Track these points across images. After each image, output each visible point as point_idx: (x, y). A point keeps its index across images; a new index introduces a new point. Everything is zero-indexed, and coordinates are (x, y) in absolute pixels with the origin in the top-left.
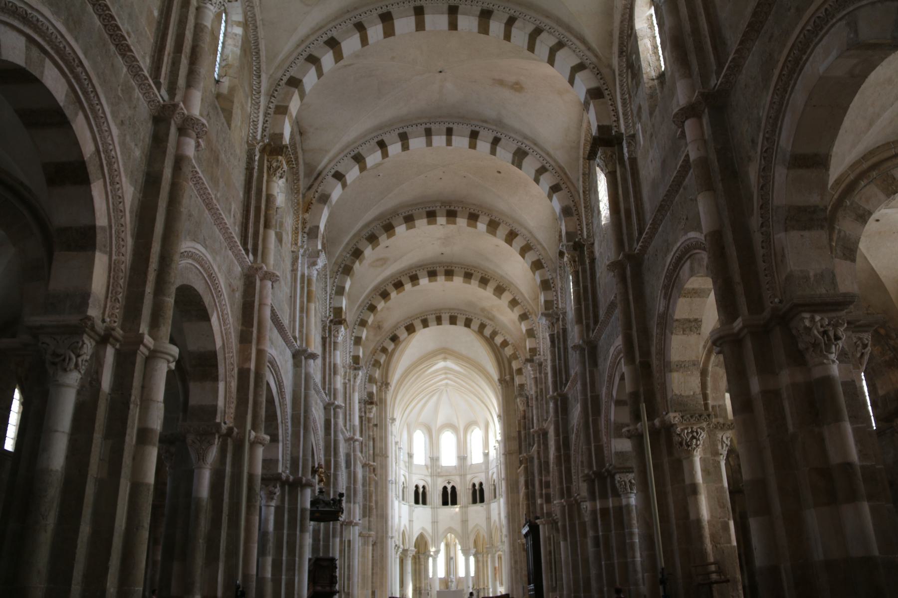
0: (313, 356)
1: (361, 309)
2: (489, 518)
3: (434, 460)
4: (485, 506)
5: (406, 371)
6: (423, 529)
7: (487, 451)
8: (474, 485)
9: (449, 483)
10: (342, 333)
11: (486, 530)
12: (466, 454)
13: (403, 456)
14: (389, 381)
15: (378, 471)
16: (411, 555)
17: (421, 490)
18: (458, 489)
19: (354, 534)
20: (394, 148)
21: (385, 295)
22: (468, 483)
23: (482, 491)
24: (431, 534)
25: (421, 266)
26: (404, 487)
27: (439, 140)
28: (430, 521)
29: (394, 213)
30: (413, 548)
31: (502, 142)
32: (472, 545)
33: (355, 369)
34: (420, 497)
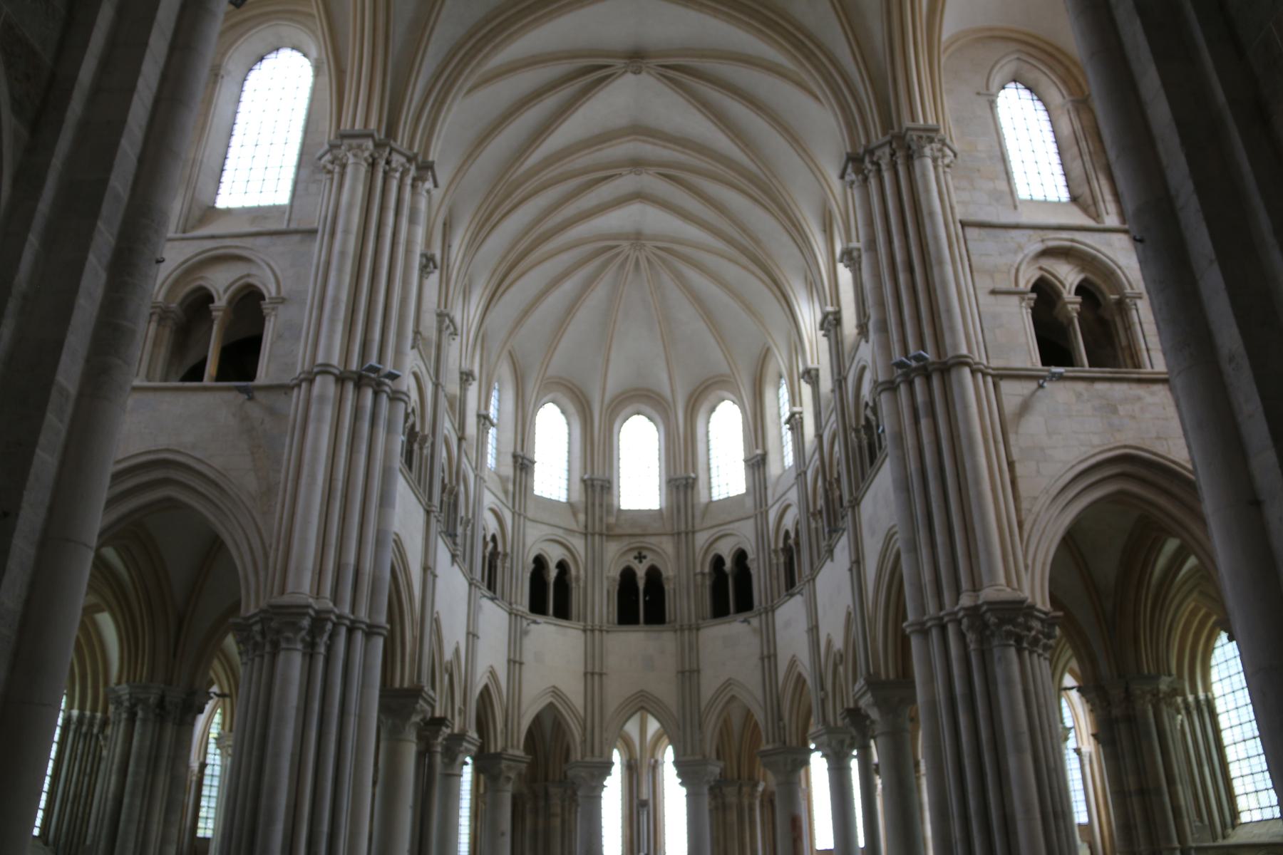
2: (769, 657)
4: (755, 622)
6: (555, 691)
7: (759, 452)
8: (718, 561)
9: (640, 558)
11: (759, 693)
12: (694, 469)
16: (512, 775)
17: (553, 573)
18: (668, 571)
22: (699, 558)
24: (582, 712)
26: (494, 553)
28: (581, 669)
30: (520, 752)
32: (710, 748)
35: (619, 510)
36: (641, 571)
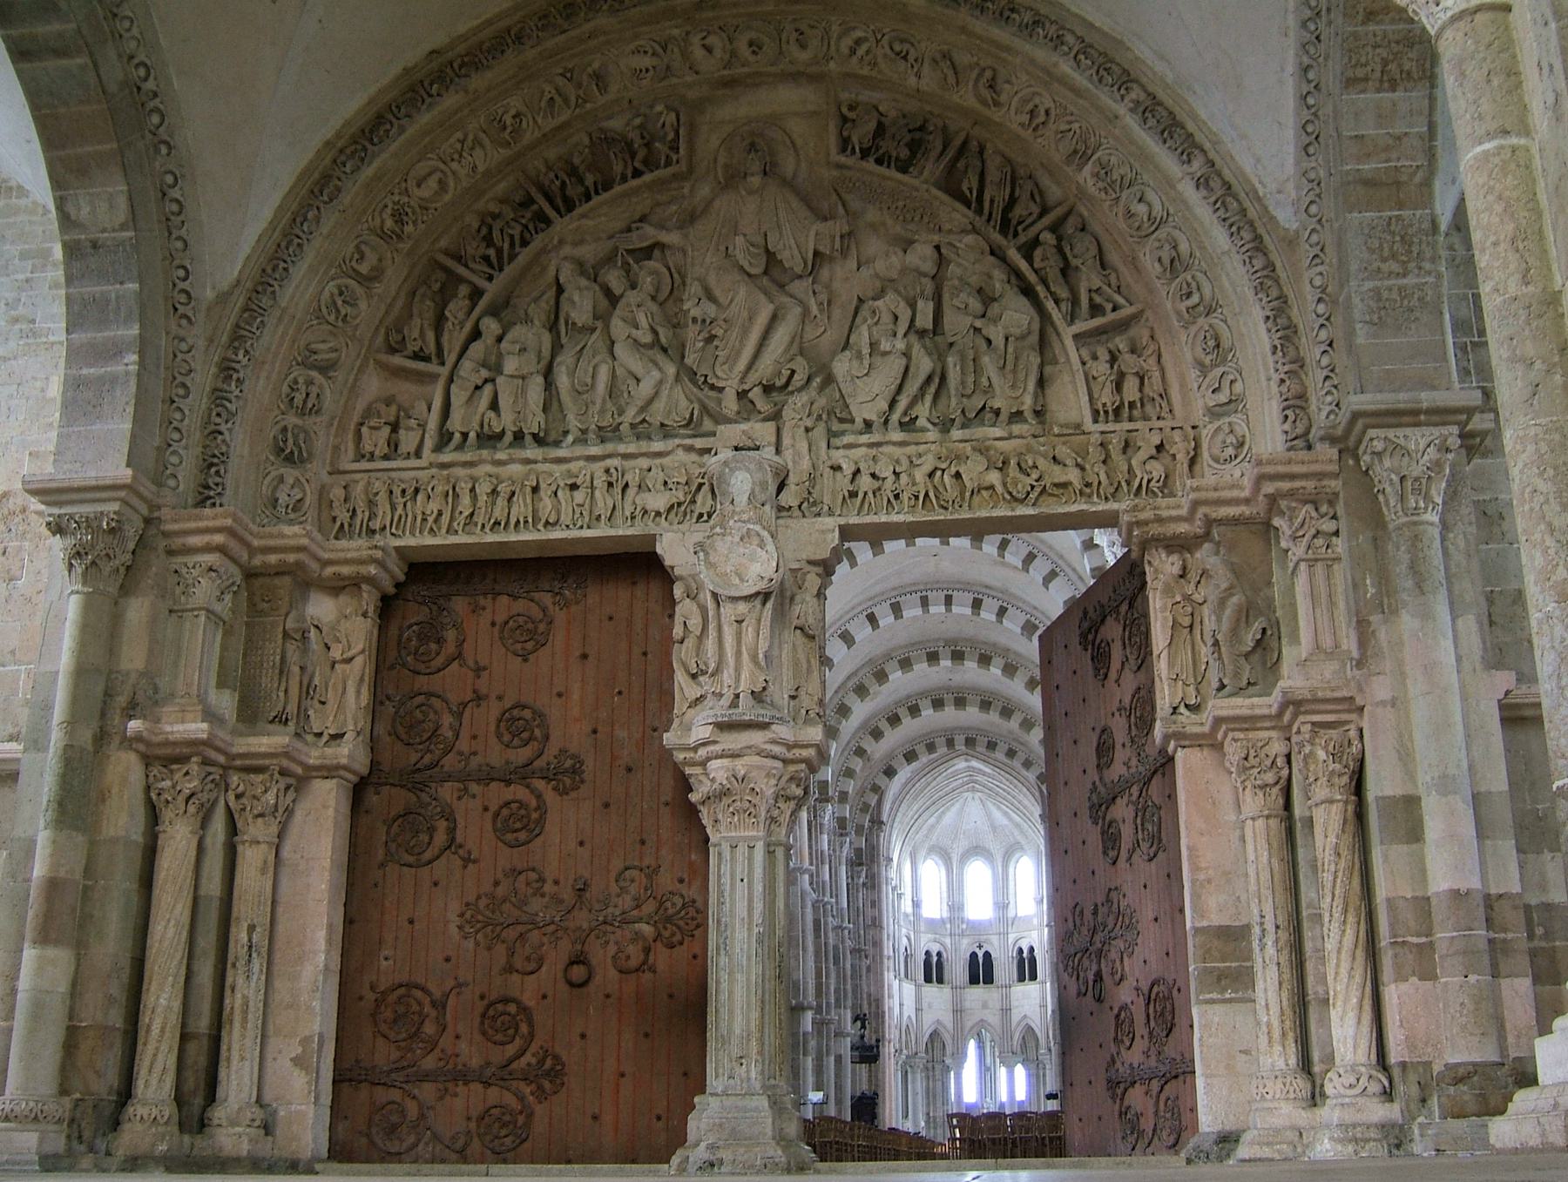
0: (806, 871)
1: (846, 753)
3: (956, 906)
5: (906, 784)
9: (980, 947)
10: (828, 813)
13: (907, 906)
14: (885, 818)
15: (871, 952)
17: (935, 959)
19: (846, 1046)
20: (886, 619)
21: (877, 734)
23: (1033, 961)
25: (923, 694)
27: (937, 609)
29: (888, 657)
31: (1011, 611)
33: (841, 835)
34: (934, 971)
35: (968, 922)
36: (980, 955)
